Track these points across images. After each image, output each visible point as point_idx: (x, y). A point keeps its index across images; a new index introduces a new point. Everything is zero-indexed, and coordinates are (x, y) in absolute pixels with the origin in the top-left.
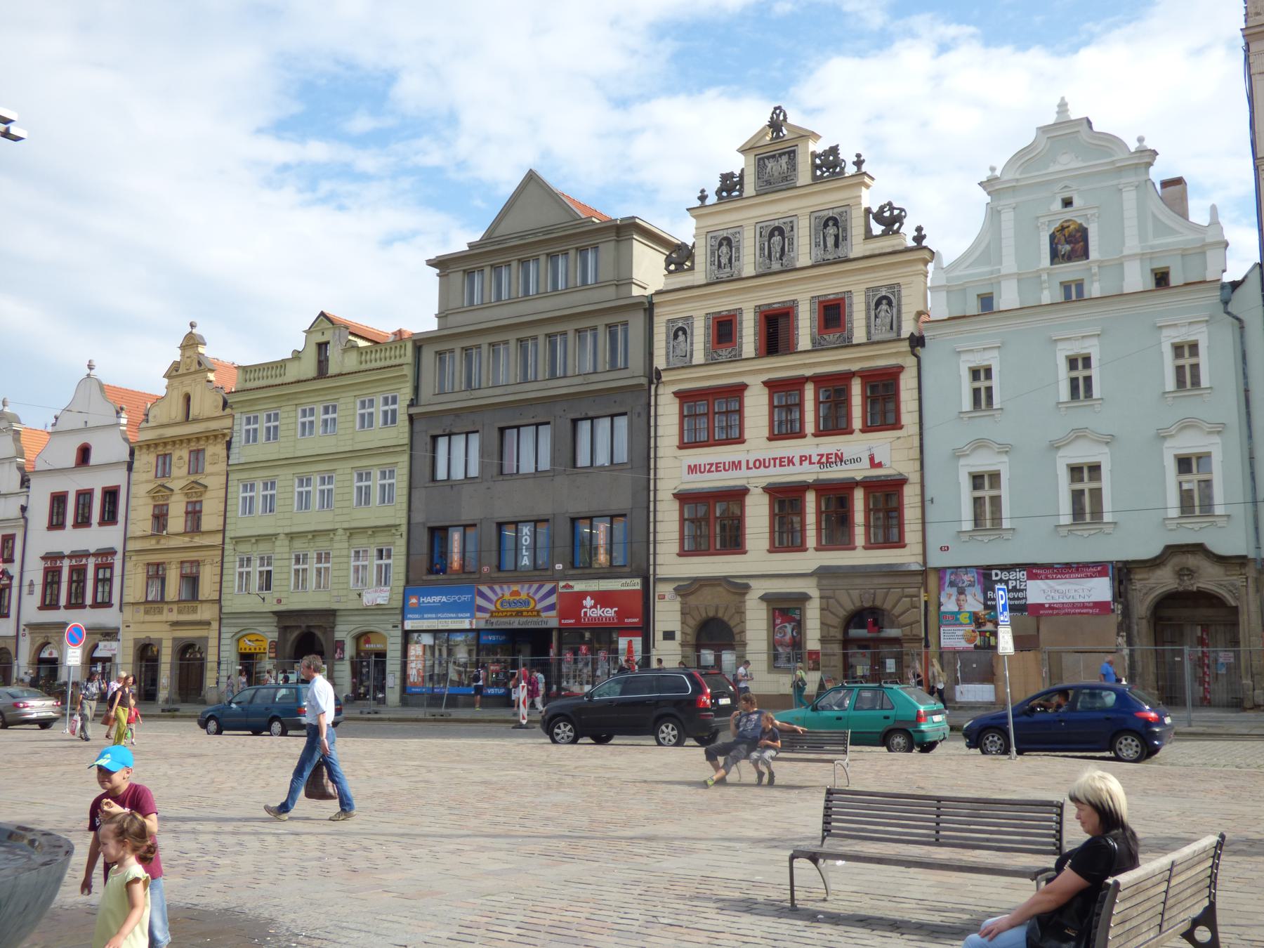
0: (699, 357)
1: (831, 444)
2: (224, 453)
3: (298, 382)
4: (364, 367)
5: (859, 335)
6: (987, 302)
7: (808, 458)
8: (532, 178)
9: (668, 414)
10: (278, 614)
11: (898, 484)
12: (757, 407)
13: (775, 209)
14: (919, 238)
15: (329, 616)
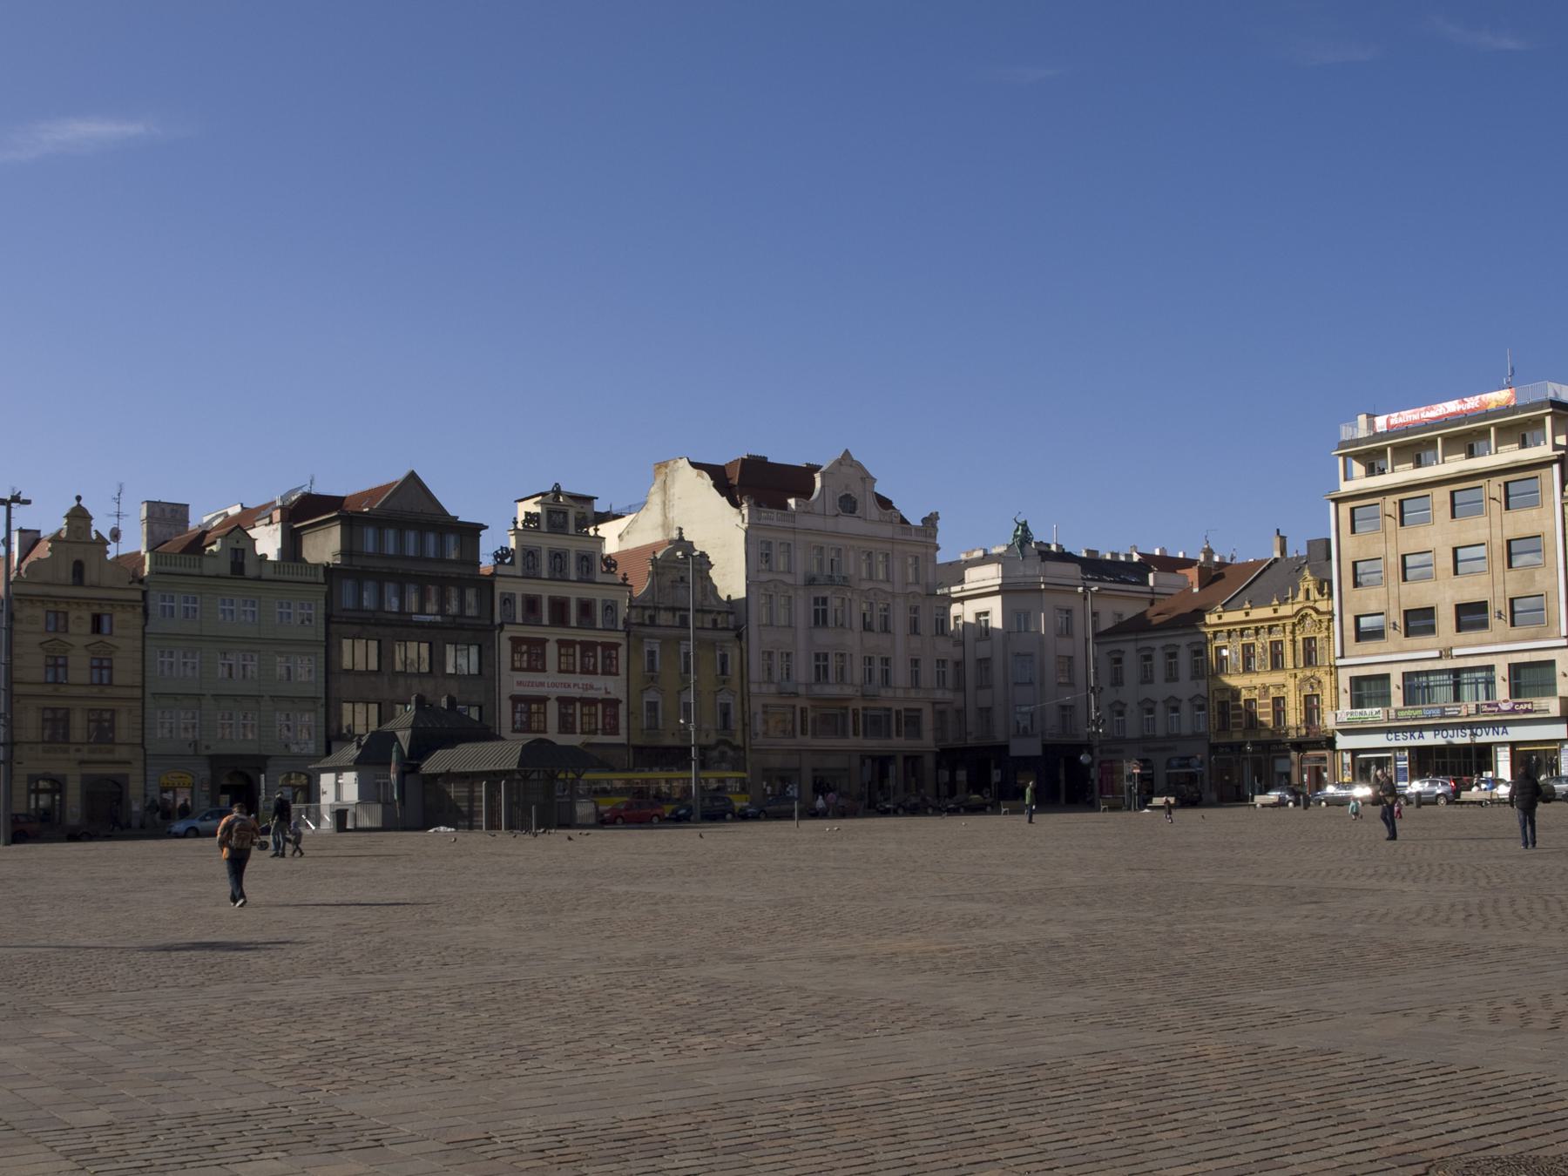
0: (519, 619)
1: (588, 679)
2: (139, 621)
3: (217, 577)
4: (277, 577)
5: (599, 625)
6: (652, 618)
7: (576, 684)
8: (413, 476)
9: (505, 647)
10: (210, 757)
11: (617, 702)
12: (552, 651)
13: (558, 542)
14: (625, 579)
15: (260, 762)
